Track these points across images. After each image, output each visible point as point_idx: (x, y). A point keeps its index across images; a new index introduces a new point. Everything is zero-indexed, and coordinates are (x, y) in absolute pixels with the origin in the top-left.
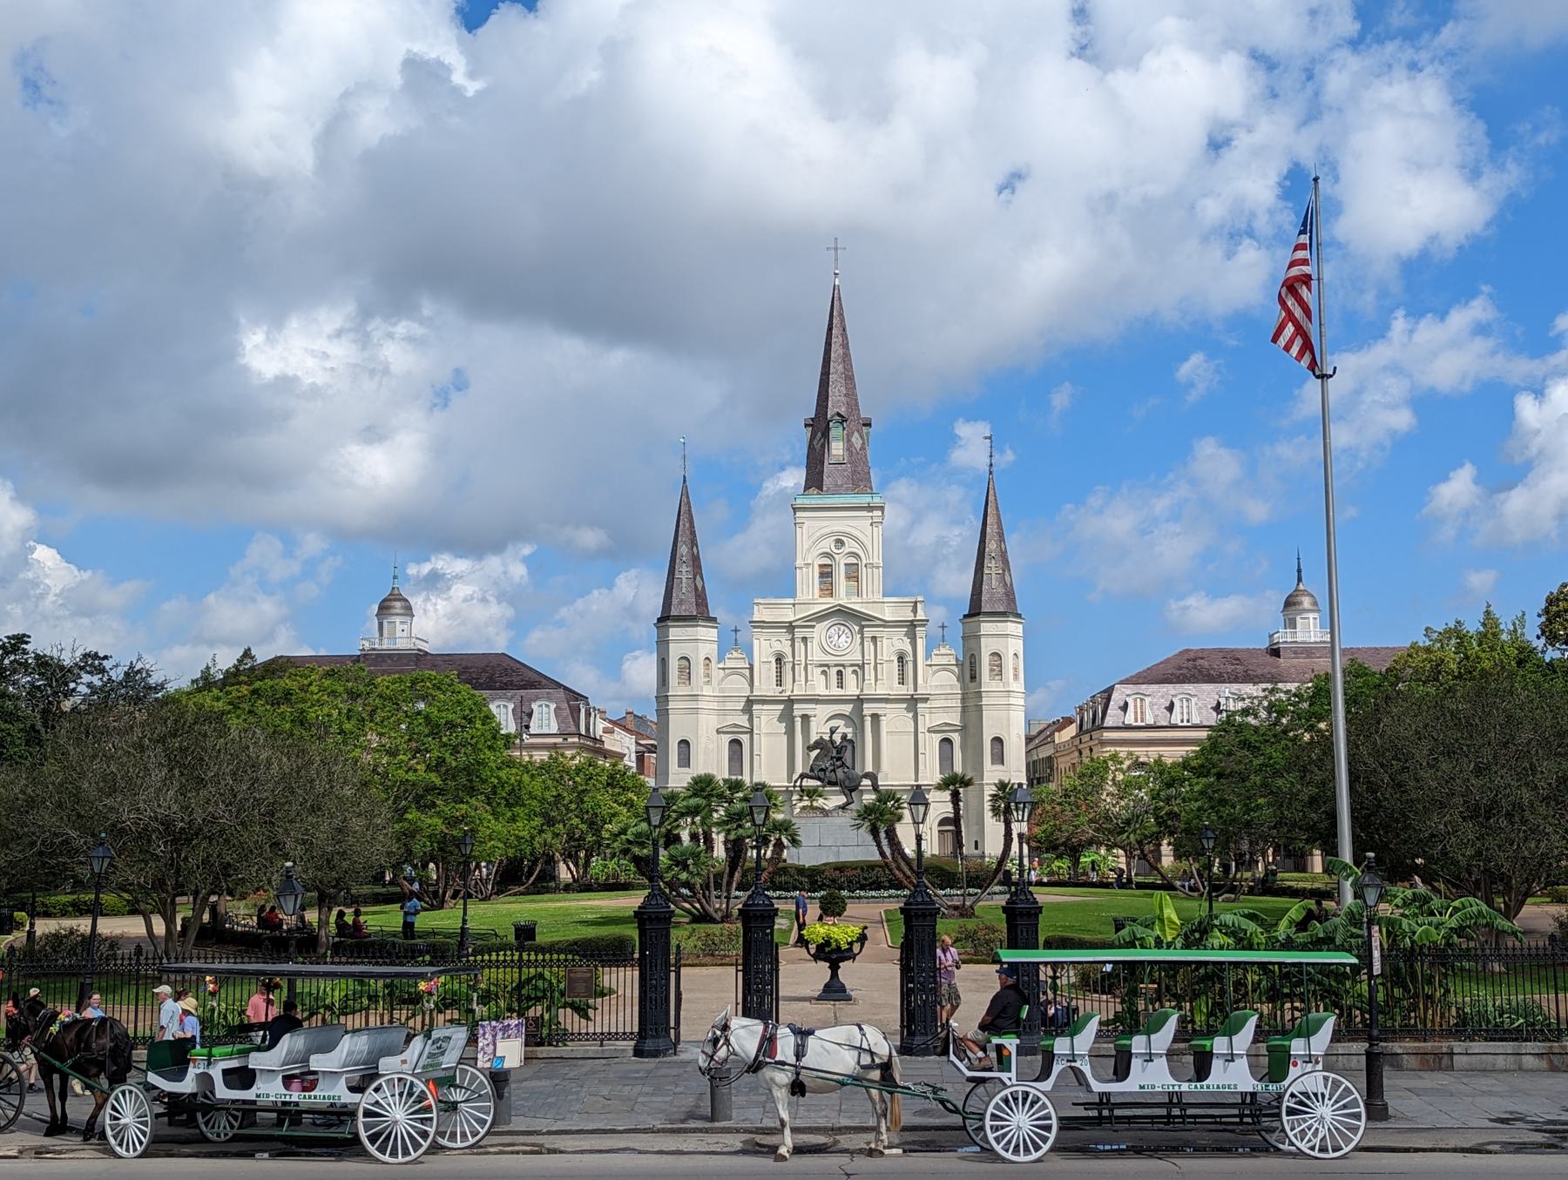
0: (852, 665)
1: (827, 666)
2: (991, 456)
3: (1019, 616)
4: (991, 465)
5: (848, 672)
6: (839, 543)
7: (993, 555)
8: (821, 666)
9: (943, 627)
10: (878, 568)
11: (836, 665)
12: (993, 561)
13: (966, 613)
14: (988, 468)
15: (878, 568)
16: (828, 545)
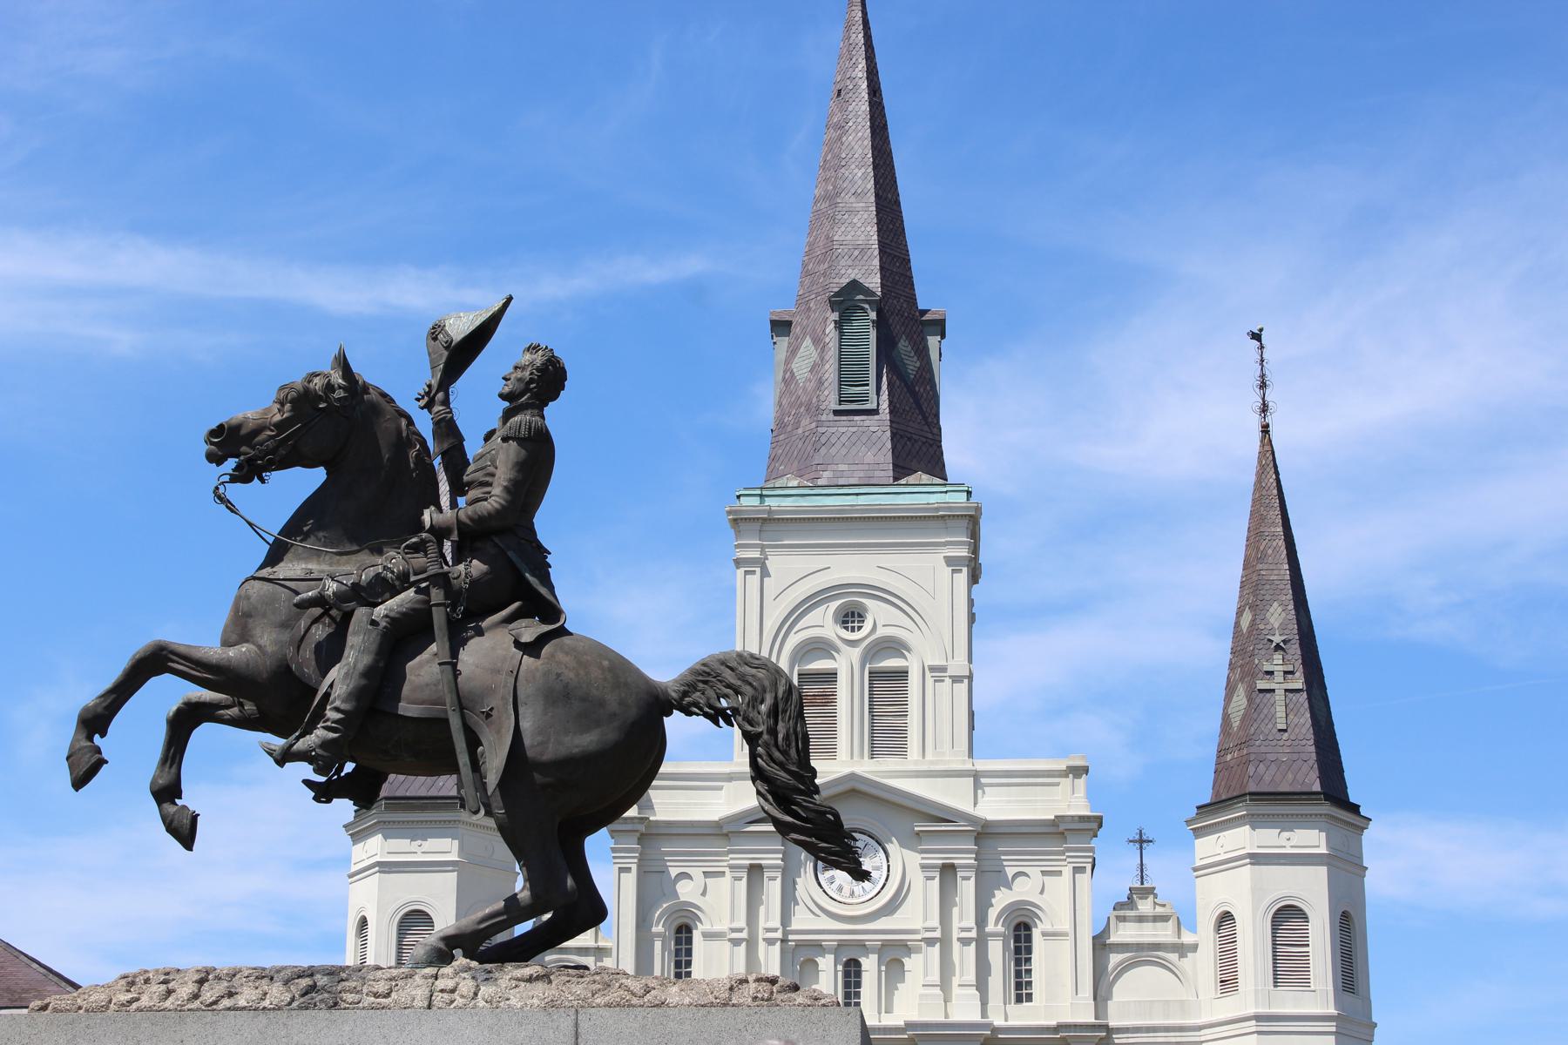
0: (886, 945)
1: (818, 947)
2: (1263, 386)
3: (1355, 809)
4: (1264, 409)
5: (869, 964)
6: (851, 617)
7: (1277, 639)
8: (800, 945)
9: (1141, 841)
10: (956, 679)
11: (842, 945)
12: (1278, 658)
13: (1208, 801)
14: (1255, 422)
15: (956, 679)
16: (822, 622)
